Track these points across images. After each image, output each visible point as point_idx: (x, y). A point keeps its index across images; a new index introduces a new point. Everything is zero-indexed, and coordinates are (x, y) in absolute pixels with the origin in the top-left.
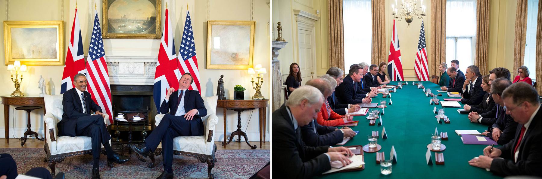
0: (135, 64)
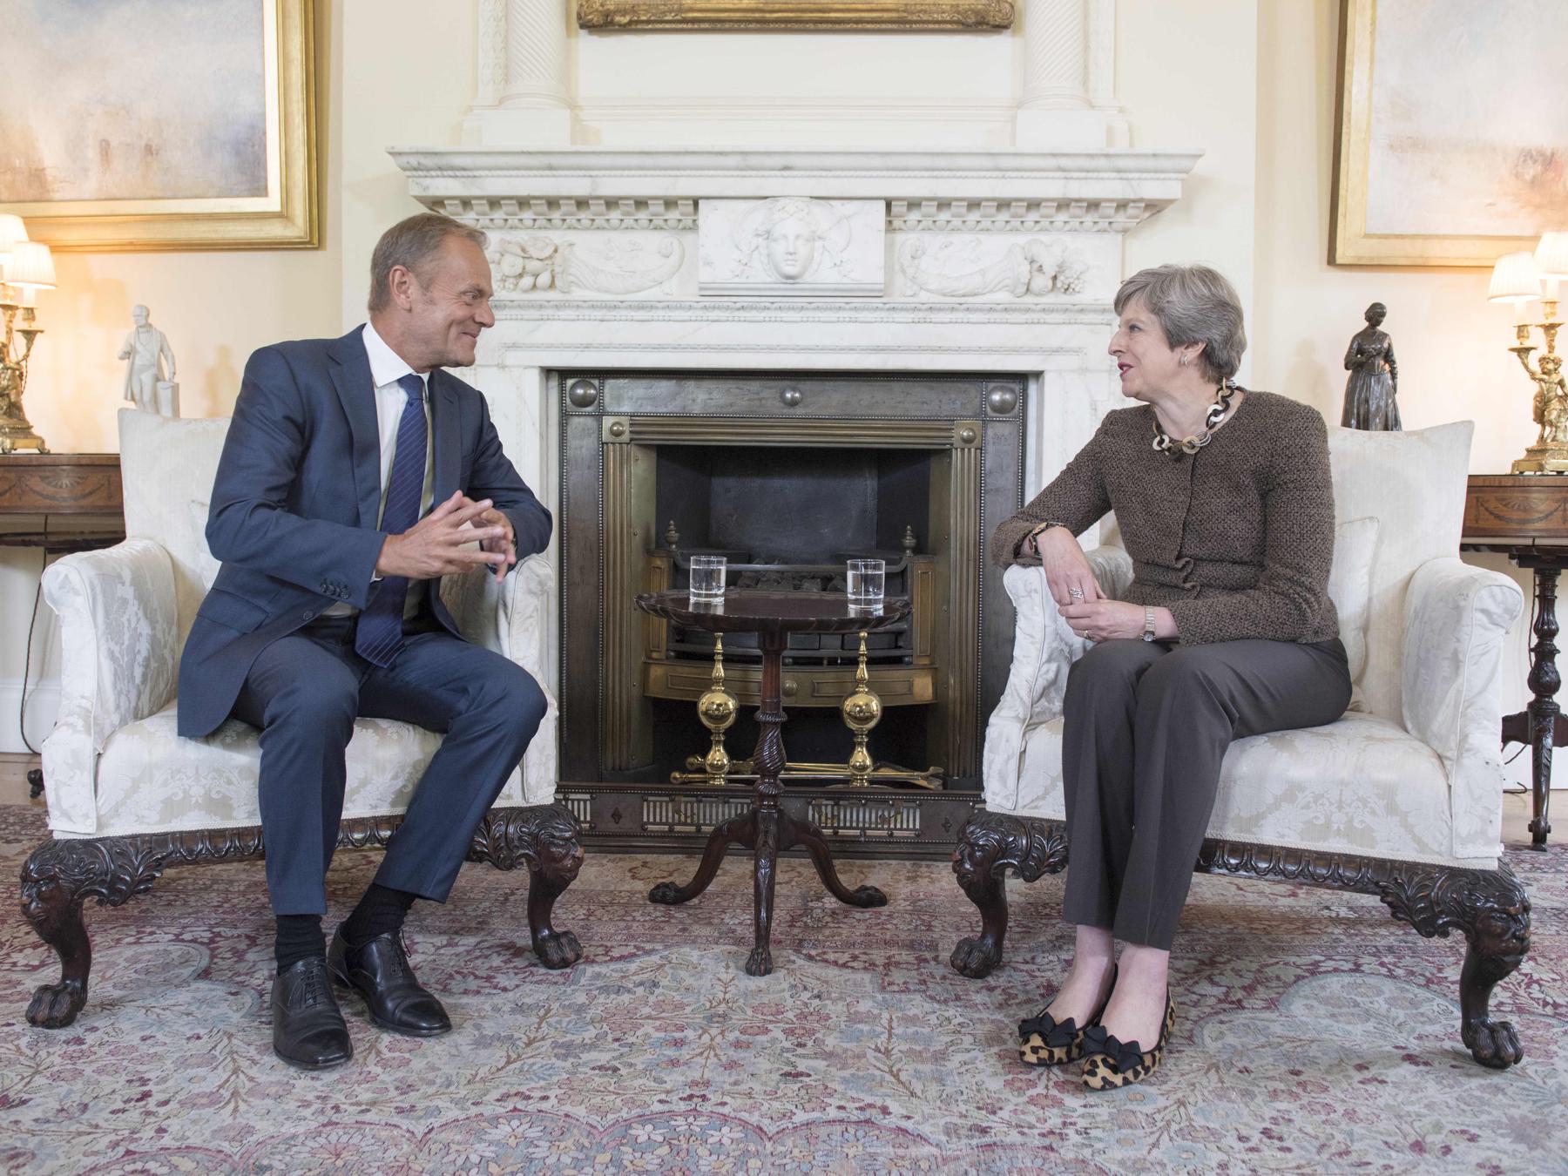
0: (819, 209)
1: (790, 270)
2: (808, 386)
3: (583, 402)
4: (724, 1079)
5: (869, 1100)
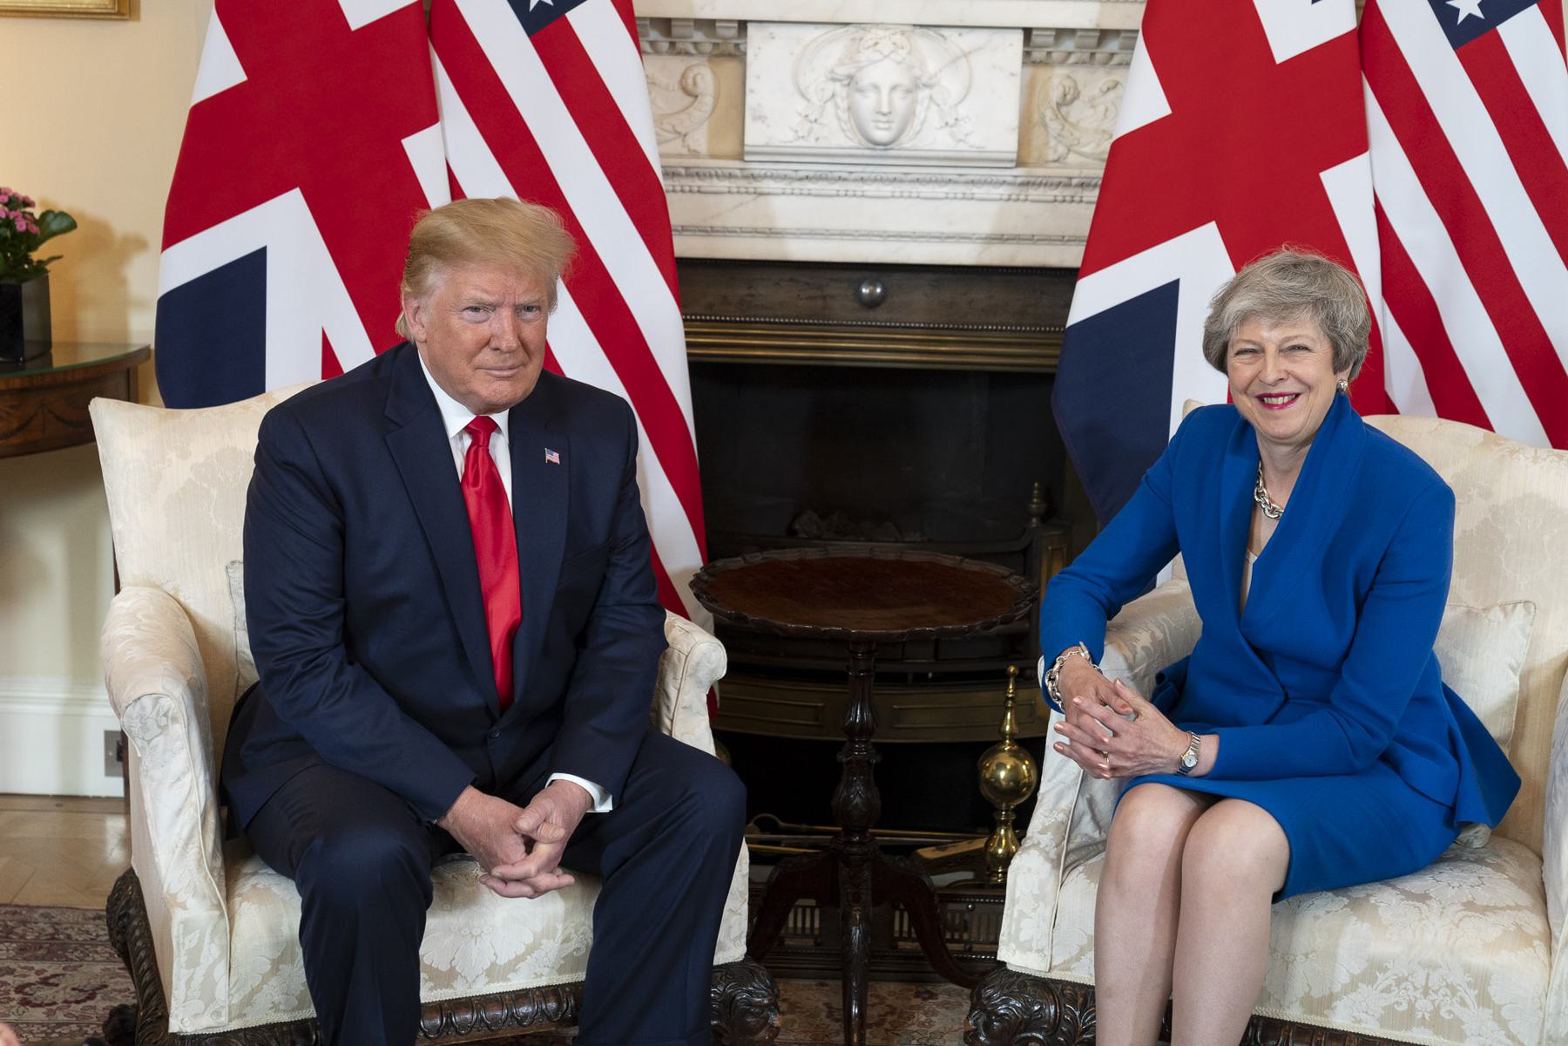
1: (881, 135)
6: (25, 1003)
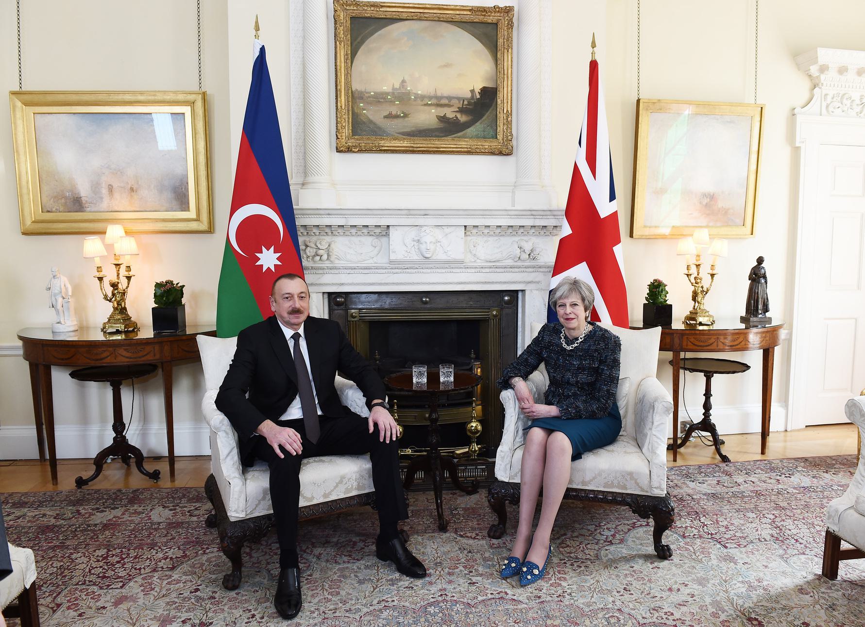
2: (431, 296)
3: (339, 304)
4: (450, 587)
5: (500, 590)
6: (191, 515)
